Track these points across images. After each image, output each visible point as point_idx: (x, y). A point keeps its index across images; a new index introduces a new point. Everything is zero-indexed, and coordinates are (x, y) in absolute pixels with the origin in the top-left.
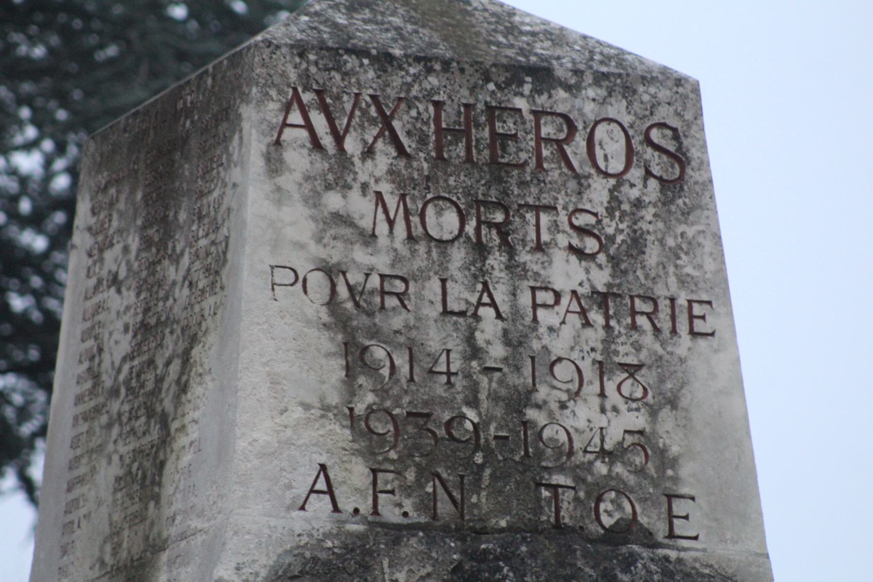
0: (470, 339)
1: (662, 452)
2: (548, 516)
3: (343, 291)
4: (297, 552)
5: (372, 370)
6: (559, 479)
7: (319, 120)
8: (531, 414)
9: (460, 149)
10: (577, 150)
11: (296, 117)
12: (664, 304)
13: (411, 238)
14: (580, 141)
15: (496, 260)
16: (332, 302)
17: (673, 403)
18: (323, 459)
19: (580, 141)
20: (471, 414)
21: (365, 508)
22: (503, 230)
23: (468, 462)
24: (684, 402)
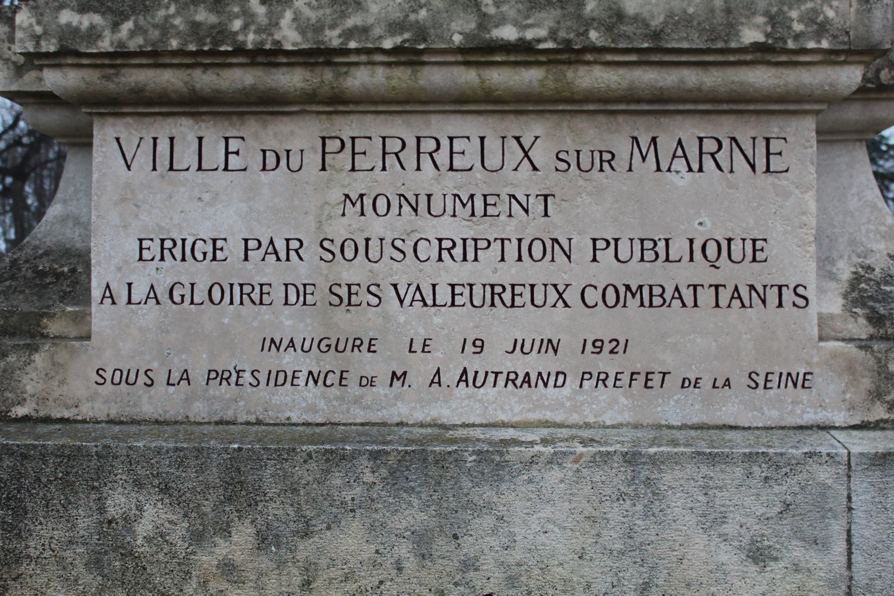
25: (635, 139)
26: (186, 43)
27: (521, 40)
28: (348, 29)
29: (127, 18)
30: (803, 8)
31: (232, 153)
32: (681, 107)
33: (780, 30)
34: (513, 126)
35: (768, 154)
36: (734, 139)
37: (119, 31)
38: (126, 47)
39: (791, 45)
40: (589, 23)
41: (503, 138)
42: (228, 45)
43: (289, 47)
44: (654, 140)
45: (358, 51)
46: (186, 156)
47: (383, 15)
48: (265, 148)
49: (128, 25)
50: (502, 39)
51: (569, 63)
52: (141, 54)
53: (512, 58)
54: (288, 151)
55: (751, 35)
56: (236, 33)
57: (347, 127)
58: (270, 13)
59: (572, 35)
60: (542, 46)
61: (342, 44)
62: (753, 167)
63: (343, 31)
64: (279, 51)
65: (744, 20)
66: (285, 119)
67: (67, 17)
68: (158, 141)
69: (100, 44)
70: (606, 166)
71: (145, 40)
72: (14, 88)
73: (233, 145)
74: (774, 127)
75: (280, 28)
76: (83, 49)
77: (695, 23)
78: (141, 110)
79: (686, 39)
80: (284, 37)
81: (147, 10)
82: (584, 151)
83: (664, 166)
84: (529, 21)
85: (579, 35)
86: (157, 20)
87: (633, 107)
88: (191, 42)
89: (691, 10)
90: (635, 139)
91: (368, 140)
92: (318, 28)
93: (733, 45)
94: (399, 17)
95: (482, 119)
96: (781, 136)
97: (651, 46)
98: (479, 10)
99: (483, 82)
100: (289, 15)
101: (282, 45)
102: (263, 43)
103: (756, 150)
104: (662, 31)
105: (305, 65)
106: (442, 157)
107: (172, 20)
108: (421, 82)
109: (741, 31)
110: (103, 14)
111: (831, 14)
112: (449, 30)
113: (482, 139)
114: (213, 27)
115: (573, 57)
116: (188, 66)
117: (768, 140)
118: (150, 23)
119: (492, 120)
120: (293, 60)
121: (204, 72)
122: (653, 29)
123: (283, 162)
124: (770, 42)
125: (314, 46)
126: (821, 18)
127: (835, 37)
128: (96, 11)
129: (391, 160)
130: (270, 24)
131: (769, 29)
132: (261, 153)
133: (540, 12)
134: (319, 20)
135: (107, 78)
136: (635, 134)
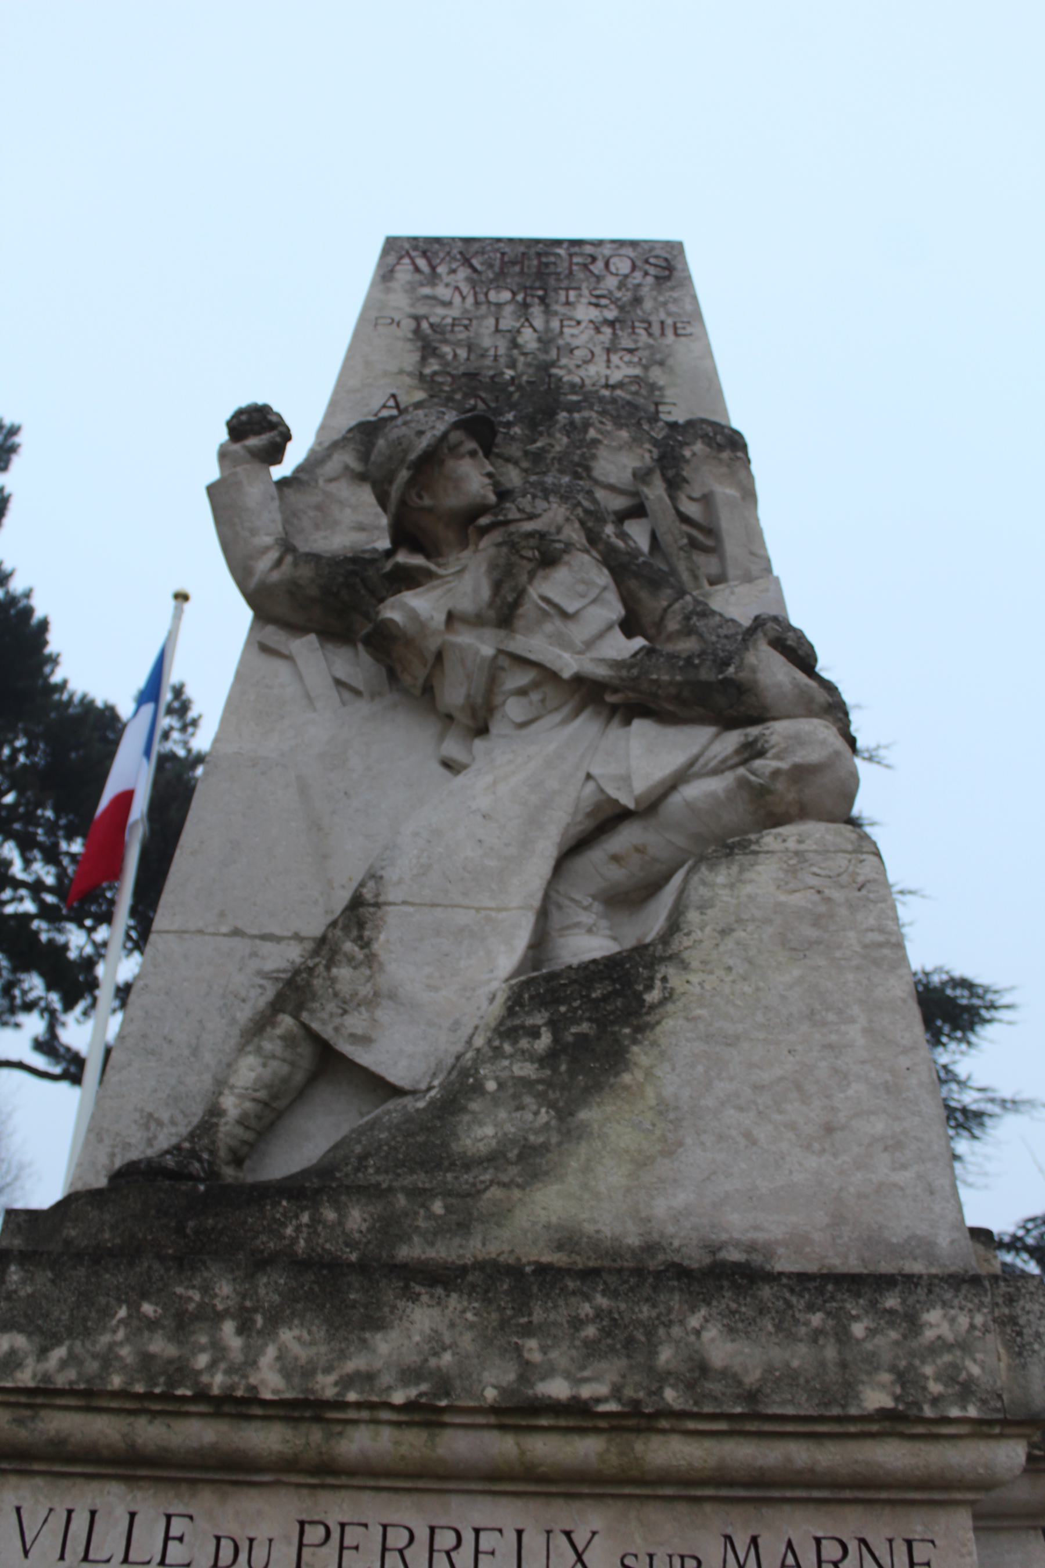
7: (422, 263)
8: (554, 371)
13: (477, 303)
18: (394, 391)
24: (670, 362)
25: (728, 1538)
26: (131, 1381)
27: (575, 1399)
28: (348, 1375)
29: (59, 1343)
30: (939, 1362)
31: (174, 1538)
32: (789, 1494)
33: (912, 1391)
36: (863, 1541)
37: (47, 1359)
38: (51, 1382)
39: (928, 1412)
40: (663, 1378)
41: (549, 1532)
42: (187, 1387)
43: (267, 1395)
44: (754, 1540)
45: (358, 1405)
47: (395, 1358)
48: (220, 1534)
49: (60, 1352)
50: (550, 1397)
51: (638, 1430)
52: (72, 1392)
53: (562, 1422)
54: (251, 1540)
56: (199, 1372)
58: (247, 1348)
59: (641, 1395)
60: (602, 1408)
61: (338, 1394)
63: (341, 1377)
64: (253, 1399)
65: (864, 1378)
66: (253, 1492)
68: (74, 1515)
69: (19, 1375)
71: (79, 1374)
73: (177, 1527)
74: (917, 1525)
75: (258, 1368)
77: (802, 1381)
78: (57, 1468)
79: (791, 1402)
80: (263, 1382)
81: (87, 1333)
82: (659, 1554)
84: (586, 1373)
85: (651, 1393)
86: (98, 1348)
87: (724, 1492)
88: (139, 1381)
89: (795, 1363)
90: (728, 1538)
91: (362, 1529)
92: (308, 1372)
93: (853, 1411)
94: (415, 1362)
95: (519, 1503)
96: (926, 1537)
97: (746, 1410)
98: (520, 1356)
99: (523, 1453)
100: (271, 1352)
101: (258, 1392)
102: (233, 1387)
103: (895, 1559)
104: (759, 1390)
105: (287, 1419)
107: (117, 1349)
108: (440, 1451)
109: (861, 1392)
110: (29, 1335)
111: (975, 1370)
112: (480, 1381)
113: (520, 1533)
114: (170, 1361)
115: (643, 1423)
117: (909, 1543)
118: (88, 1351)
119: (534, 1506)
120: (271, 1412)
121: (150, 1422)
122: (747, 1387)
123: (243, 1557)
124: (901, 1407)
125: (301, 1396)
126: (963, 1376)
127: (984, 1402)
128: (21, 1330)
130: (245, 1363)
131: (898, 1390)
132: (214, 1541)
133: (599, 1361)
134: (310, 1361)
135: (20, 1422)
136: (729, 1531)
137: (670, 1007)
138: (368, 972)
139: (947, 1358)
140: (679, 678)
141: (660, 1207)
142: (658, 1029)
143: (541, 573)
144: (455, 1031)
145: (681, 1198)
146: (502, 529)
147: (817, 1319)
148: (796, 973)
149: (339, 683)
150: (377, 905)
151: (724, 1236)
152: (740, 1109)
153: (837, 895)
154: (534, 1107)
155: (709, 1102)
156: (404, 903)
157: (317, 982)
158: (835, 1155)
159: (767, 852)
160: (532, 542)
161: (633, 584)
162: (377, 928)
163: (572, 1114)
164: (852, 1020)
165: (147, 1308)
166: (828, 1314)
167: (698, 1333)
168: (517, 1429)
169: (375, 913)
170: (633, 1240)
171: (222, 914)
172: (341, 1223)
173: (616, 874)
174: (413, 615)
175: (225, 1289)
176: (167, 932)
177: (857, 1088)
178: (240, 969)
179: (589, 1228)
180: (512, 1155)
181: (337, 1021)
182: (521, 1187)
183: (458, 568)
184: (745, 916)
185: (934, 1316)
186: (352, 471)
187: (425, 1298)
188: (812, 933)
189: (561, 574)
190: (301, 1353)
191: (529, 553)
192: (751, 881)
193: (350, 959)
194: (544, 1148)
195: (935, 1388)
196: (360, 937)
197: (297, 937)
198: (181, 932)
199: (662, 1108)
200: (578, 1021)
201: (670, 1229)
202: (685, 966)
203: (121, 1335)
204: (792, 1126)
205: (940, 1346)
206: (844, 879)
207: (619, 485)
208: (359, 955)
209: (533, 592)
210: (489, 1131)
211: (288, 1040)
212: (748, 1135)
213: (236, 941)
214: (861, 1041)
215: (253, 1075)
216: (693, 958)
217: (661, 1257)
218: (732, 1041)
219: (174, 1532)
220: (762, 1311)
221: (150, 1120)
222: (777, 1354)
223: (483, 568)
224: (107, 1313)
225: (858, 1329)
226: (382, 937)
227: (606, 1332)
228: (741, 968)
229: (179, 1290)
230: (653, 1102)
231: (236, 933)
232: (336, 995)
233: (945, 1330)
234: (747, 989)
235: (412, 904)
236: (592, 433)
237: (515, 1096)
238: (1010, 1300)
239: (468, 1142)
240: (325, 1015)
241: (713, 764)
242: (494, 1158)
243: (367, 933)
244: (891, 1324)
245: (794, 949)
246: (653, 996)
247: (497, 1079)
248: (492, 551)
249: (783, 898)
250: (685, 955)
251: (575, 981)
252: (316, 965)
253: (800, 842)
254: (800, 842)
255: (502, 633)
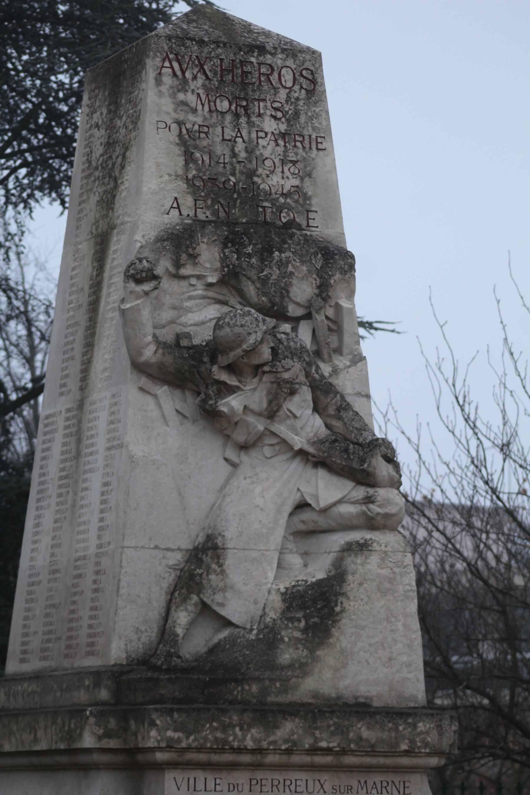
0: (233, 150)
1: (305, 194)
2: (261, 218)
3: (184, 131)
4: (166, 230)
5: (195, 161)
6: (266, 204)
7: (176, 65)
8: (256, 179)
9: (230, 77)
10: (274, 78)
11: (167, 64)
12: (307, 138)
13: (210, 111)
14: (276, 74)
15: (243, 120)
16: (180, 135)
17: (310, 175)
18: (176, 195)
19: (276, 74)
20: (233, 179)
21: (192, 214)
22: (246, 108)
23: (231, 197)
24: (314, 175)
25: (359, 781)
34: (317, 775)
35: (404, 787)
36: (393, 782)
39: (417, 751)
40: (350, 741)
43: (249, 747)
44: (366, 782)
46: (200, 786)
49: (192, 738)
51: (342, 755)
53: (324, 753)
55: (404, 747)
56: (230, 742)
57: (259, 775)
58: (243, 735)
59: (345, 746)
62: (399, 792)
67: (169, 733)
70: (349, 791)
72: (98, 746)
74: (406, 778)
76: (176, 746)
83: (369, 792)
87: (360, 769)
89: (384, 737)
90: (359, 781)
92: (260, 741)
93: (398, 750)
100: (249, 736)
102: (240, 745)
105: (251, 753)
106: (293, 787)
108: (291, 761)
110: (183, 733)
111: (429, 739)
113: (307, 780)
114: (223, 739)
116: (209, 752)
117: (404, 782)
123: (236, 788)
127: (430, 748)
129: (275, 788)
137: (344, 615)
138: (222, 577)
139: (423, 736)
140: (344, 463)
141: (342, 684)
142: (340, 622)
143: (288, 398)
144: (256, 604)
145: (348, 682)
146: (274, 375)
147: (390, 725)
148: (383, 602)
149: (177, 411)
150: (224, 549)
151: (359, 694)
152: (365, 652)
153: (397, 570)
154: (302, 649)
155: (356, 650)
156: (234, 548)
157: (204, 581)
158: (391, 668)
159: (375, 551)
160: (288, 385)
161: (319, 393)
162: (224, 559)
163: (314, 652)
164: (399, 621)
165: (215, 724)
166: (394, 724)
167: (360, 729)
168: (311, 755)
169: (223, 553)
170: (334, 695)
171: (150, 539)
172: (250, 690)
173: (302, 527)
174: (232, 409)
175: (235, 718)
176: (130, 547)
177: (399, 645)
178: (160, 564)
179: (321, 691)
180: (297, 666)
181: (212, 597)
182: (302, 678)
183: (252, 387)
184: (367, 578)
185: (420, 725)
186: (170, 272)
187: (289, 719)
188: (388, 585)
189: (297, 398)
190: (258, 736)
191: (286, 391)
192: (369, 563)
193: (215, 571)
194: (306, 664)
195: (419, 744)
196: (218, 562)
197: (179, 549)
198: (136, 548)
199: (342, 651)
200: (313, 617)
201: (344, 692)
202: (348, 598)
203: (208, 732)
204: (380, 658)
205: (421, 733)
206: (400, 563)
207: (301, 303)
208: (218, 570)
209: (285, 407)
210: (287, 656)
211: (195, 605)
212: (367, 661)
213: (157, 551)
214: (402, 629)
215: (186, 620)
216: (351, 594)
217: (342, 700)
218: (363, 628)
219: (218, 782)
220: (376, 723)
221: (137, 630)
222: (380, 735)
223: (265, 392)
224: (203, 726)
225: (401, 728)
226: (227, 563)
227: (336, 729)
228: (366, 599)
229: (223, 718)
230: (339, 649)
231: (156, 547)
232: (211, 586)
233: (423, 729)
234: (368, 608)
235: (237, 549)
236: (290, 268)
237: (295, 644)
238: (441, 720)
239: (281, 660)
240: (208, 595)
241: (352, 500)
242: (291, 666)
243: (221, 561)
244: (410, 727)
245: (382, 592)
246: (338, 609)
247: (288, 636)
248: (269, 385)
249: (380, 571)
250: (348, 594)
251: (310, 600)
252: (202, 573)
253: (386, 546)
254: (386, 546)
255: (269, 421)
